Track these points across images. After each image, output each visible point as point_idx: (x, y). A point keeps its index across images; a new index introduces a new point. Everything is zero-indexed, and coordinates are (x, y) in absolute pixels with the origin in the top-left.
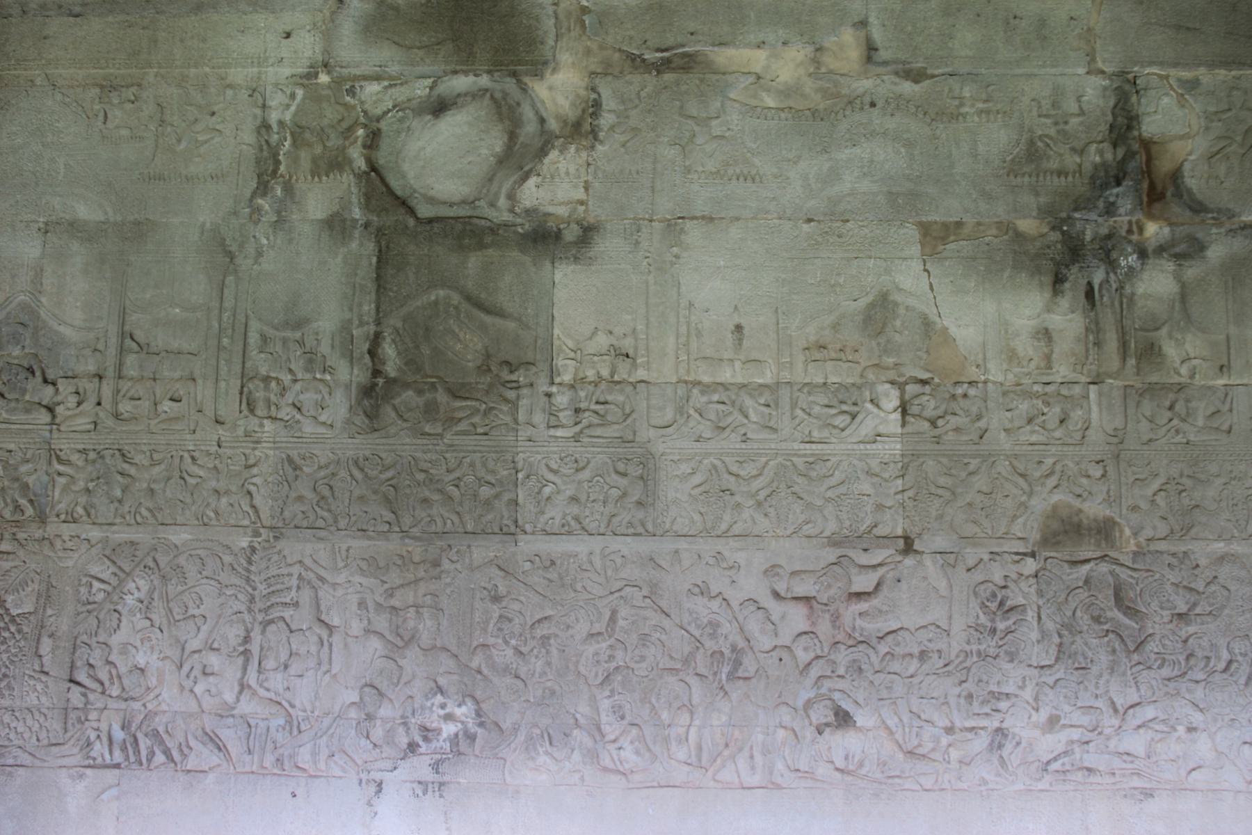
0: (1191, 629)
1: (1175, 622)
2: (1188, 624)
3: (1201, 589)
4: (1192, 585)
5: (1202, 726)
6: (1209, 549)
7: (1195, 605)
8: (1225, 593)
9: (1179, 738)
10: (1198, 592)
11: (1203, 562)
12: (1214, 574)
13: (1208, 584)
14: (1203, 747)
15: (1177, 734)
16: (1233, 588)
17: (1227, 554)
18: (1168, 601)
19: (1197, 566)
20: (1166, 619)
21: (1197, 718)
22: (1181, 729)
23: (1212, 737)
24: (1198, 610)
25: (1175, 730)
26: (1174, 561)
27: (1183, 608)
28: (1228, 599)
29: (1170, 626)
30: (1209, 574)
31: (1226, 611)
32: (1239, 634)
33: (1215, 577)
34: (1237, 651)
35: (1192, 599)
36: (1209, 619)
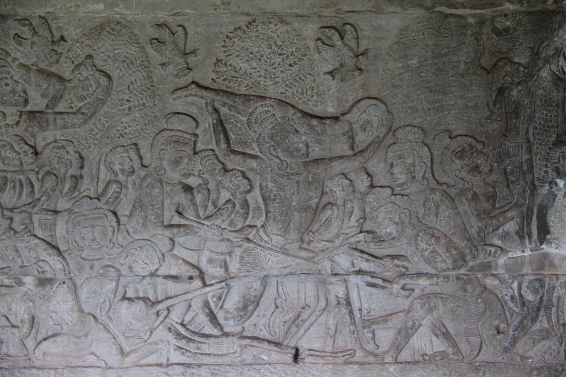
0: (49, 135)
1: (23, 125)
2: (43, 128)
3: (67, 75)
4: (53, 69)
5: (61, 276)
6: (81, 12)
7: (56, 99)
8: (103, 81)
9: (26, 294)
10: (60, 79)
11: (72, 33)
12: (87, 51)
13: (78, 66)
14: (60, 306)
15: (23, 289)
16: (114, 74)
17: (108, 21)
18: (13, 91)
19: (62, 38)
20: (10, 120)
21: (53, 264)
22: (29, 281)
23: (75, 290)
24: (61, 107)
25: (20, 283)
26: (26, 32)
27: (38, 102)
28: (108, 91)
29: (17, 130)
30: (80, 52)
31: (105, 108)
32: (122, 141)
33: (90, 57)
34: (117, 167)
35: (51, 91)
36: (78, 119)
